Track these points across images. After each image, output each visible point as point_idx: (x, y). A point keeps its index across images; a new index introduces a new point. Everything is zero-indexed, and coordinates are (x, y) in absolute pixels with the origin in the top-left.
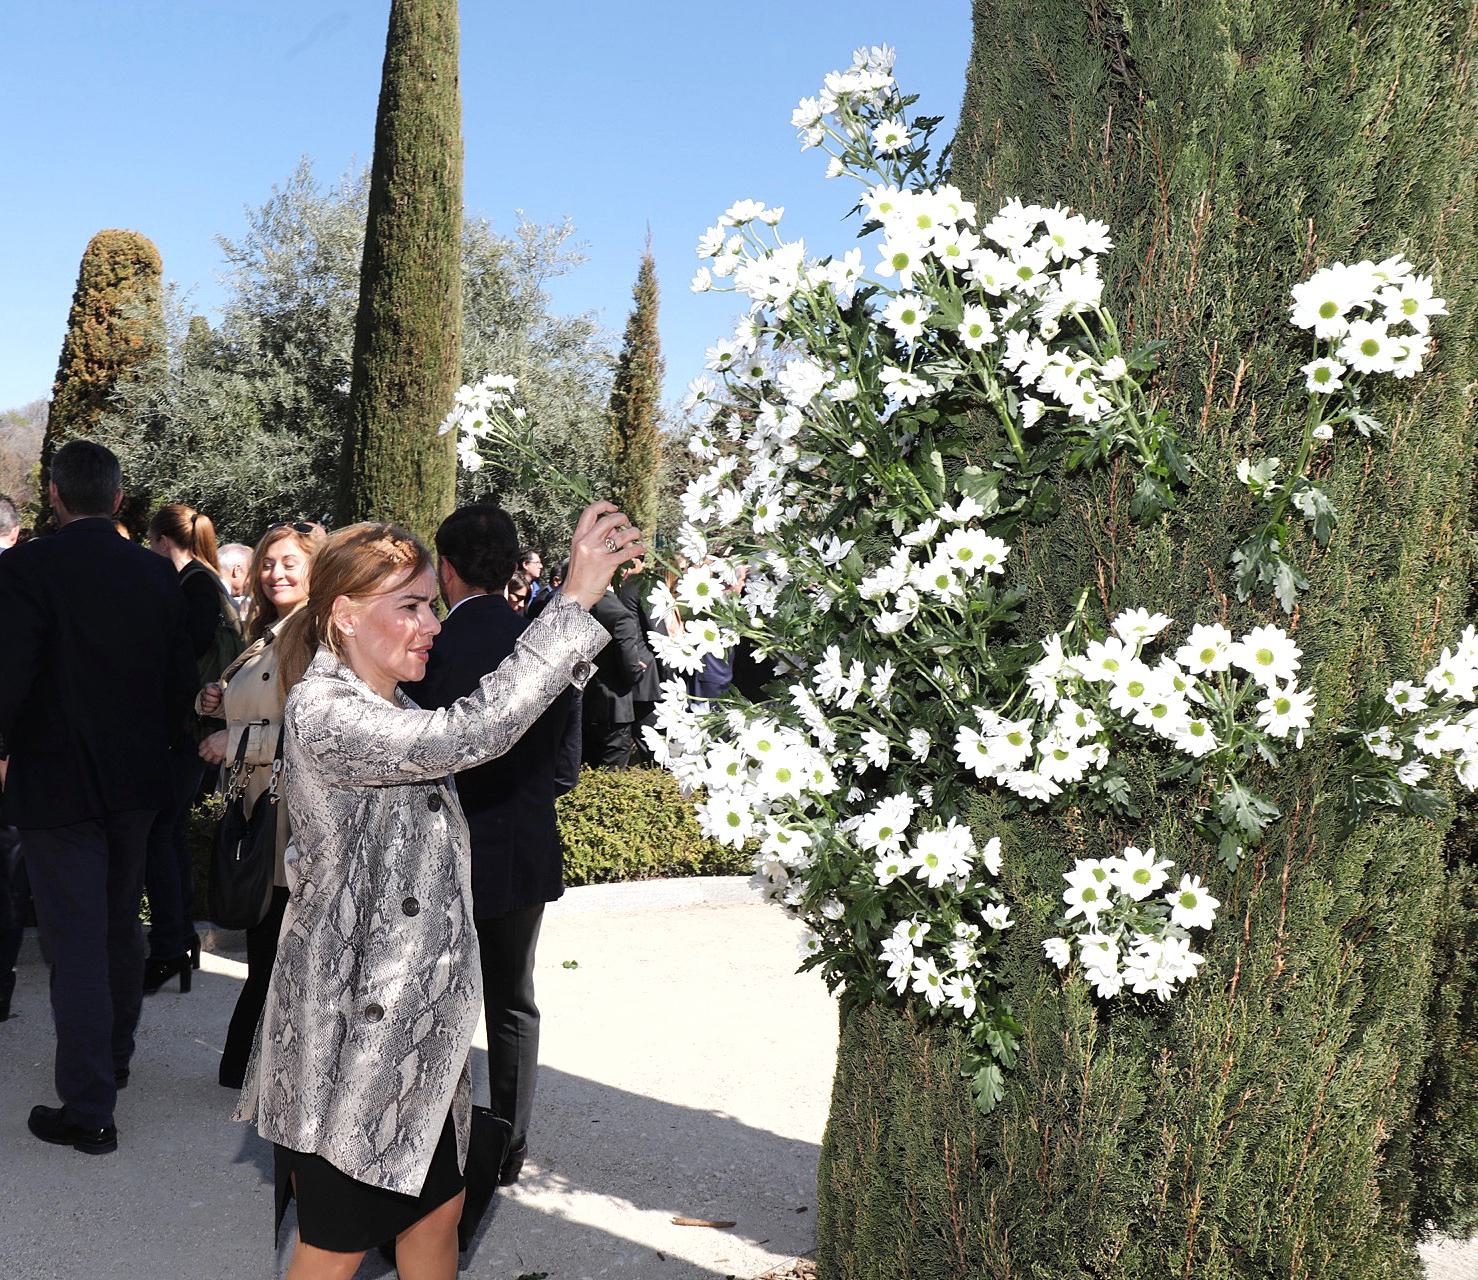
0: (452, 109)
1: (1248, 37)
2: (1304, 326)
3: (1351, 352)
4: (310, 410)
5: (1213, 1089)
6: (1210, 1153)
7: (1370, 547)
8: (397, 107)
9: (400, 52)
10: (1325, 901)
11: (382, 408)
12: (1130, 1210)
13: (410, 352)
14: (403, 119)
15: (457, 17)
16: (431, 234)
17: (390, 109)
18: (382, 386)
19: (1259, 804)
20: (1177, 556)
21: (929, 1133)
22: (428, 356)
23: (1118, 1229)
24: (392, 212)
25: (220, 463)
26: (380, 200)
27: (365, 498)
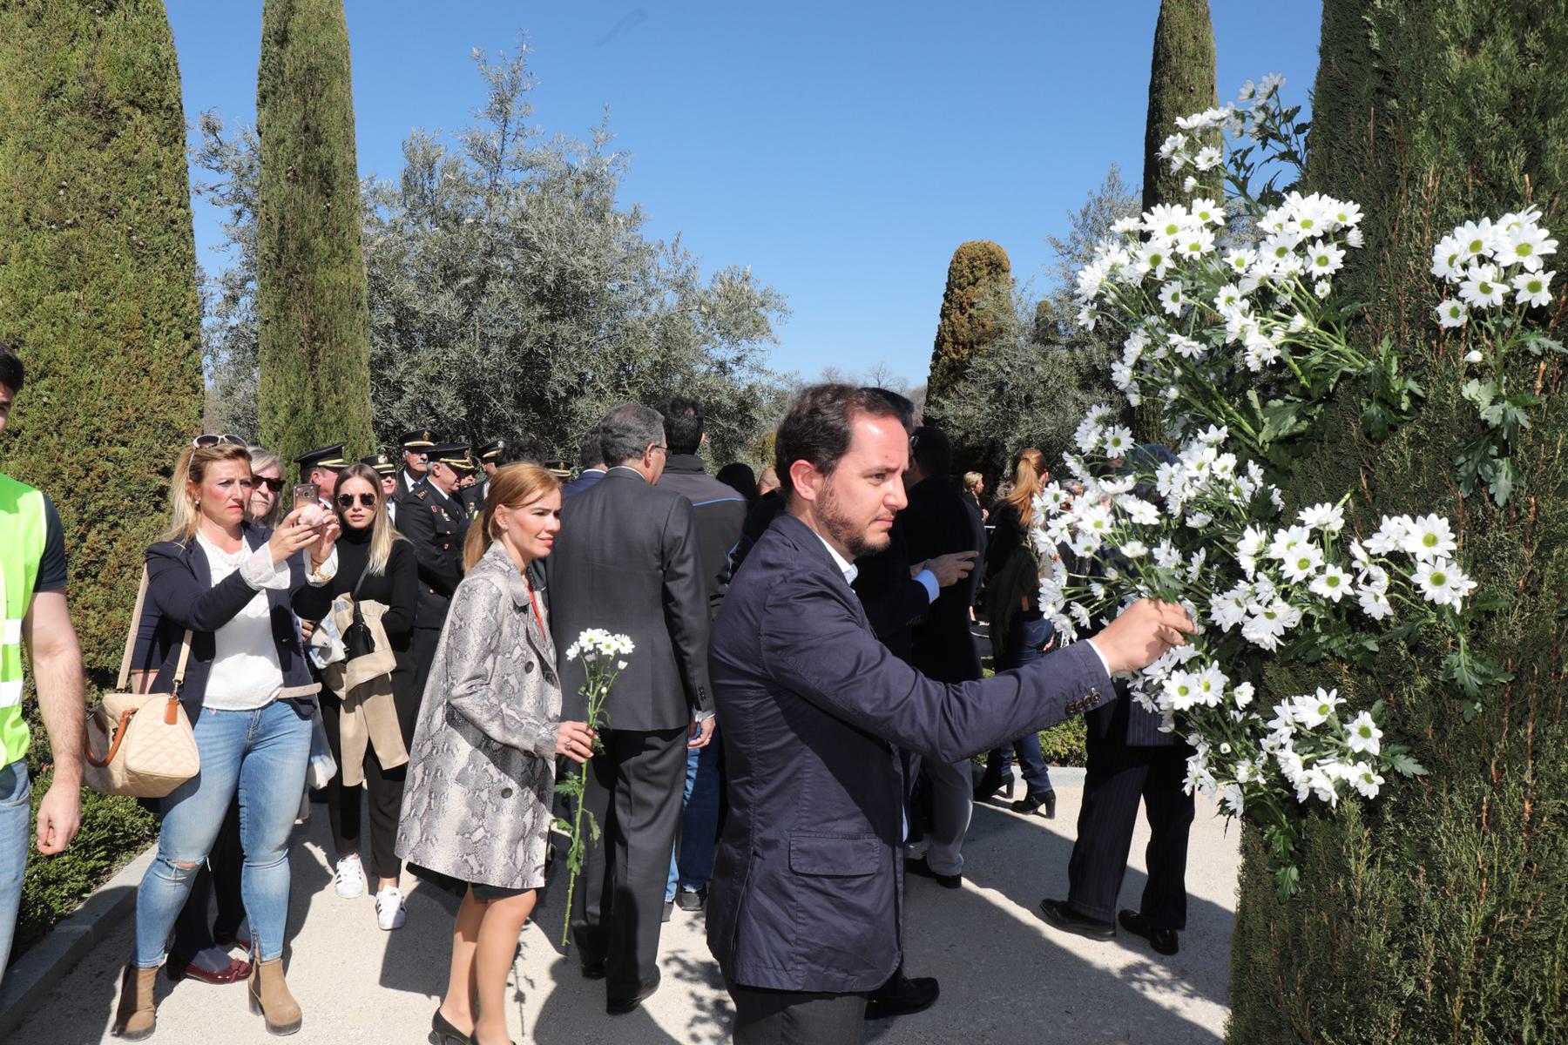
2: (1440, 275)
3: (1470, 292)
5: (1469, 909)
6: (1467, 963)
8: (1161, 119)
15: (1213, 34)
19: (1477, 666)
20: (1416, 462)
25: (1048, 418)
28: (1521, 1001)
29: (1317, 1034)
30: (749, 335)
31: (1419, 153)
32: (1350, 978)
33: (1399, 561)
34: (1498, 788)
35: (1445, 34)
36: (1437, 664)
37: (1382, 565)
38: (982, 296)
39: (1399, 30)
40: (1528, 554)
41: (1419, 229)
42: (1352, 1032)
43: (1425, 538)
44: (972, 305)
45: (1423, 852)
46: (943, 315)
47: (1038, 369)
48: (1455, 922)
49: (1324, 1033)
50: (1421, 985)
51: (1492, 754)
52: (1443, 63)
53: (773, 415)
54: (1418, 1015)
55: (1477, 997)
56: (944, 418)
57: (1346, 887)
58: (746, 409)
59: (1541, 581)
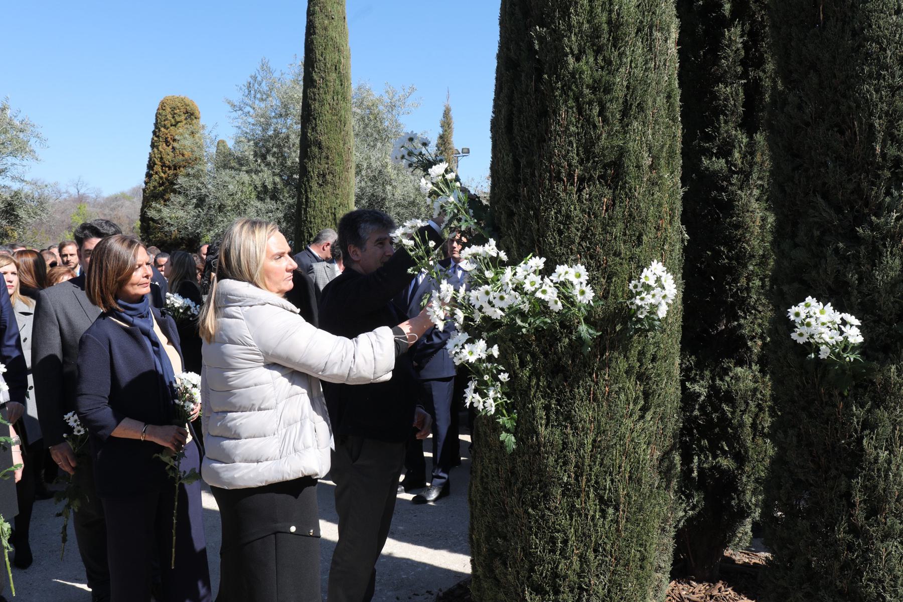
0: (343, 33)
1: (576, 52)
6: (587, 461)
7: (631, 236)
8: (315, 33)
9: (315, 5)
10: (623, 365)
11: (315, 187)
12: (560, 484)
13: (327, 158)
14: (318, 39)
16: (335, 98)
17: (311, 34)
18: (314, 175)
19: (590, 331)
21: (494, 466)
22: (337, 160)
23: (557, 492)
24: (315, 87)
26: (309, 82)
27: (309, 232)
29: (526, 512)
30: (13, 154)
31: (558, 102)
33: (563, 286)
34: (597, 383)
36: (571, 333)
37: (557, 287)
38: (181, 132)
39: (547, 43)
40: (603, 281)
41: (560, 136)
42: (543, 506)
43: (574, 274)
44: (174, 140)
45: (569, 417)
46: (153, 146)
47: (231, 187)
48: (582, 445)
49: (530, 510)
50: (569, 477)
51: (593, 369)
52: (566, 62)
53: (36, 213)
54: (569, 490)
55: (590, 475)
56: (162, 218)
58: (13, 210)
59: (608, 293)
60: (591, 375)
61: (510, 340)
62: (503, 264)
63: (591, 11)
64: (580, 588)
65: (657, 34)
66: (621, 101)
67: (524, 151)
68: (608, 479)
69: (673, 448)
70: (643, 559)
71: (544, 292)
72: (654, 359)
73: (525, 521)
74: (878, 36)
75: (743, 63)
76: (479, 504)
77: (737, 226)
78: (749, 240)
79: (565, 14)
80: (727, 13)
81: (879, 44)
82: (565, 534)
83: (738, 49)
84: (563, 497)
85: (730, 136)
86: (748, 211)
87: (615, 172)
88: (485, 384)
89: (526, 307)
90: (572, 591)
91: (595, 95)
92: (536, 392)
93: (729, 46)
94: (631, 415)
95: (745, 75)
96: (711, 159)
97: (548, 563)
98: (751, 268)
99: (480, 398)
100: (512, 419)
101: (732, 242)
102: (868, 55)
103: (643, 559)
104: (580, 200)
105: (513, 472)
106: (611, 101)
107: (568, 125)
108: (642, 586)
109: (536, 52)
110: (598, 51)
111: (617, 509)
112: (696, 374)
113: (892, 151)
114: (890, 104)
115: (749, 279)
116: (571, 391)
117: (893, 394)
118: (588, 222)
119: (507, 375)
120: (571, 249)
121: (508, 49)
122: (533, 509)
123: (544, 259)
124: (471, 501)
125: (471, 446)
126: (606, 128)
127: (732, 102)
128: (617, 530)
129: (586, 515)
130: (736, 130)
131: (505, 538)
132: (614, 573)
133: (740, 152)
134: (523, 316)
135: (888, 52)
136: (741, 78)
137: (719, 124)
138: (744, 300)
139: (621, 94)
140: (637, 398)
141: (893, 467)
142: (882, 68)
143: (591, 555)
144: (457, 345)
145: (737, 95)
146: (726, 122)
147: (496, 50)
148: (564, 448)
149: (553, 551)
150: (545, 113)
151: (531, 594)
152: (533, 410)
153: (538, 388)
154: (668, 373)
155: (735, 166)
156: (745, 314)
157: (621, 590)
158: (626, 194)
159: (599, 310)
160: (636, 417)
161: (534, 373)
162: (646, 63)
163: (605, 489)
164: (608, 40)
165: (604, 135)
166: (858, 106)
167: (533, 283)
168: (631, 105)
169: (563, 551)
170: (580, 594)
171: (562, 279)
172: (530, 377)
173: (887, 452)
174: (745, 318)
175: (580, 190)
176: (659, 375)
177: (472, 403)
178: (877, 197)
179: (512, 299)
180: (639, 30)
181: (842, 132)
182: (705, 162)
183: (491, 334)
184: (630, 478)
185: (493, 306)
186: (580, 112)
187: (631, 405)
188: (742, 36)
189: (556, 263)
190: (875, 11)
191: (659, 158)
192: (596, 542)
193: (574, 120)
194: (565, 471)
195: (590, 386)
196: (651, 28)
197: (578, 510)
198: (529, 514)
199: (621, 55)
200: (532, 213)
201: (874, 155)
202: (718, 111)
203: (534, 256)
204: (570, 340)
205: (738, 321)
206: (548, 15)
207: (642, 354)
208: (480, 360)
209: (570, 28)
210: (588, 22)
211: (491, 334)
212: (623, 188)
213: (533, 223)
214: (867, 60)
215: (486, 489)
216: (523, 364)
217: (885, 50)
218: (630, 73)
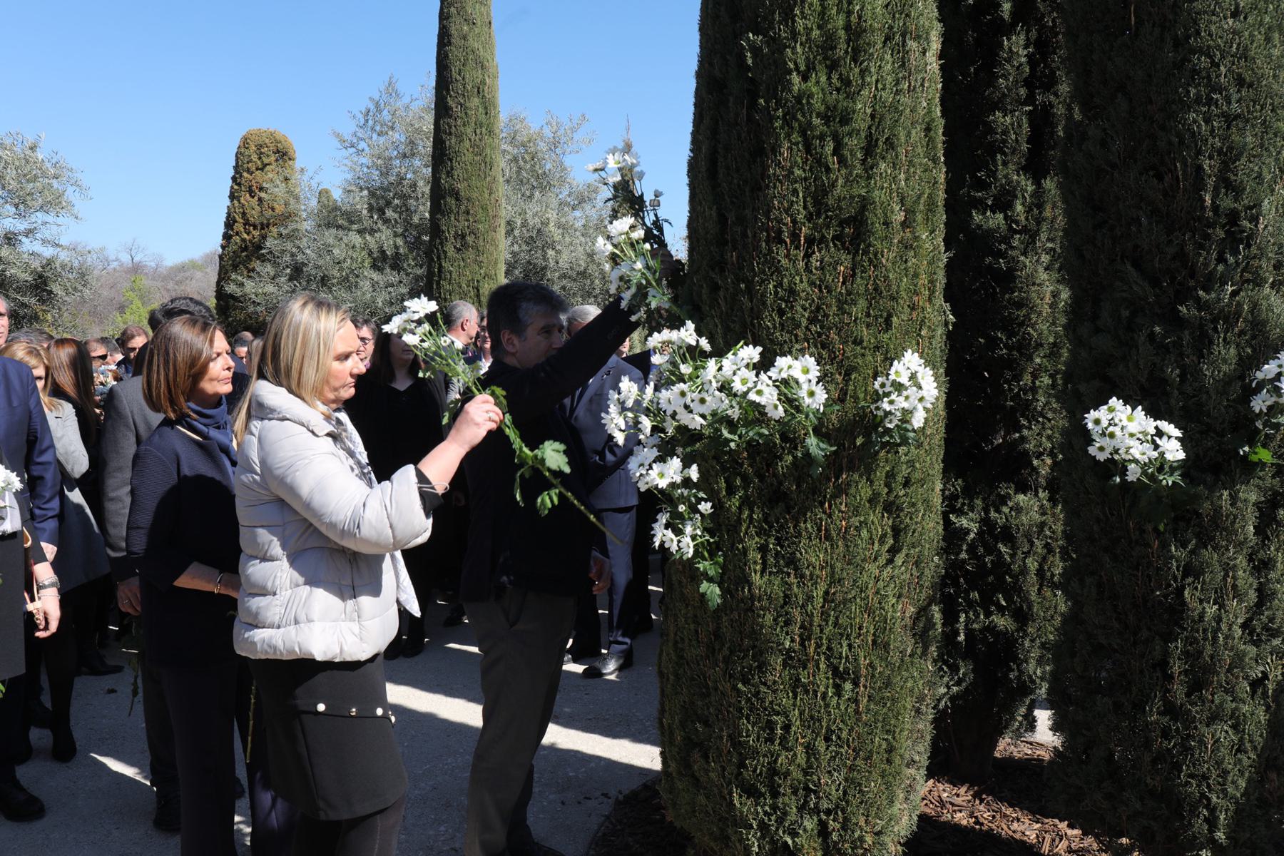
0: (488, 43)
1: (803, 68)
4: (406, 255)
6: (817, 620)
7: (876, 317)
8: (450, 44)
9: (450, 5)
10: (865, 491)
11: (451, 252)
12: (780, 651)
13: (468, 213)
14: (454, 52)
16: (478, 131)
17: (445, 45)
18: (450, 235)
19: (822, 445)
22: (481, 216)
24: (450, 117)
26: (442, 109)
28: (842, 635)
29: (735, 688)
32: (754, 647)
34: (830, 516)
35: (792, 65)
37: (777, 387)
40: (839, 378)
41: (781, 182)
44: (261, 189)
45: (792, 562)
47: (336, 252)
48: (810, 598)
49: (740, 685)
50: (793, 641)
52: (790, 82)
53: (75, 289)
54: (792, 658)
55: (821, 639)
57: (749, 590)
59: (846, 394)
60: (822, 504)
61: (714, 458)
62: (705, 355)
63: (823, 13)
64: (807, 789)
65: (912, 44)
66: (863, 134)
67: (732, 202)
68: (845, 643)
69: (931, 600)
70: (890, 750)
71: (759, 393)
72: (907, 483)
73: (733, 700)
74: (1209, 47)
75: (1028, 83)
76: (672, 677)
77: (1020, 304)
78: (1036, 323)
79: (788, 16)
80: (1006, 16)
81: (1210, 57)
82: (787, 717)
83: (1021, 65)
84: (785, 668)
85: (1010, 182)
86: (1034, 284)
87: (855, 232)
88: (680, 516)
89: (735, 413)
90: (795, 793)
91: (829, 127)
92: (748, 527)
93: (1008, 60)
94: (876, 558)
95: (1030, 99)
96: (984, 214)
97: (765, 756)
98: (1038, 360)
99: (673, 536)
100: (716, 563)
101: (1012, 326)
102: (1195, 72)
103: (890, 750)
104: (808, 269)
105: (717, 634)
106: (850, 135)
107: (792, 167)
108: (888, 786)
109: (749, 68)
110: (833, 67)
111: (856, 684)
112: (963, 504)
113: (1227, 203)
114: (1225, 139)
115: (1035, 376)
116: (795, 527)
117: (1225, 529)
118: (819, 298)
119: (709, 505)
120: (796, 336)
121: (711, 64)
122: (744, 684)
123: (759, 349)
124: (661, 674)
125: (662, 597)
126: (843, 171)
127: (1013, 137)
128: (857, 712)
129: (815, 692)
130: (1018, 175)
131: (706, 723)
132: (851, 769)
133: (1023, 204)
134: (732, 425)
135: (1222, 68)
136: (1025, 103)
137: (996, 166)
138: (1028, 404)
139: (864, 126)
140: (884, 536)
141: (1224, 626)
142: (1214, 90)
143: (821, 745)
144: (642, 465)
145: (1020, 126)
146: (1005, 164)
147: (693, 65)
148: (785, 603)
149: (770, 740)
150: (761, 151)
151: (741, 797)
152: (745, 551)
153: (751, 522)
154: (926, 502)
155: (1017, 223)
156: (1030, 422)
157: (860, 791)
158: (870, 261)
159: (833, 417)
160: (882, 561)
161: (745, 501)
162: (897, 84)
163: (840, 658)
164: (846, 52)
165: (840, 181)
166: (1181, 142)
167: (744, 381)
168: (877, 140)
169: (784, 740)
170: (806, 797)
171: (784, 375)
172: (740, 508)
173: (1216, 607)
174: (1030, 428)
175: (808, 256)
176: (913, 505)
177: (662, 543)
178: (1206, 265)
179: (717, 401)
180: (888, 39)
181: (1160, 177)
182: (977, 217)
183: (688, 449)
184: (874, 642)
185: (691, 412)
186: (808, 148)
187: (876, 546)
188: (1026, 47)
189: (776, 355)
190: (1205, 12)
191: (914, 212)
192: (828, 728)
193: (799, 160)
194: (787, 634)
195: (821, 519)
196: (903, 35)
197: (804, 686)
198: (738, 690)
199: (863, 72)
200: (743, 286)
201: (1203, 208)
202: (994, 149)
203: (747, 345)
204: (795, 457)
205: (1020, 432)
206: (765, 19)
207: (891, 476)
208: (673, 485)
209: (794, 35)
210: (819, 27)
211: (688, 449)
212: (866, 252)
213: (744, 299)
214: (1194, 79)
215: (682, 657)
216: (731, 491)
217: (1218, 66)
218: (875, 96)
